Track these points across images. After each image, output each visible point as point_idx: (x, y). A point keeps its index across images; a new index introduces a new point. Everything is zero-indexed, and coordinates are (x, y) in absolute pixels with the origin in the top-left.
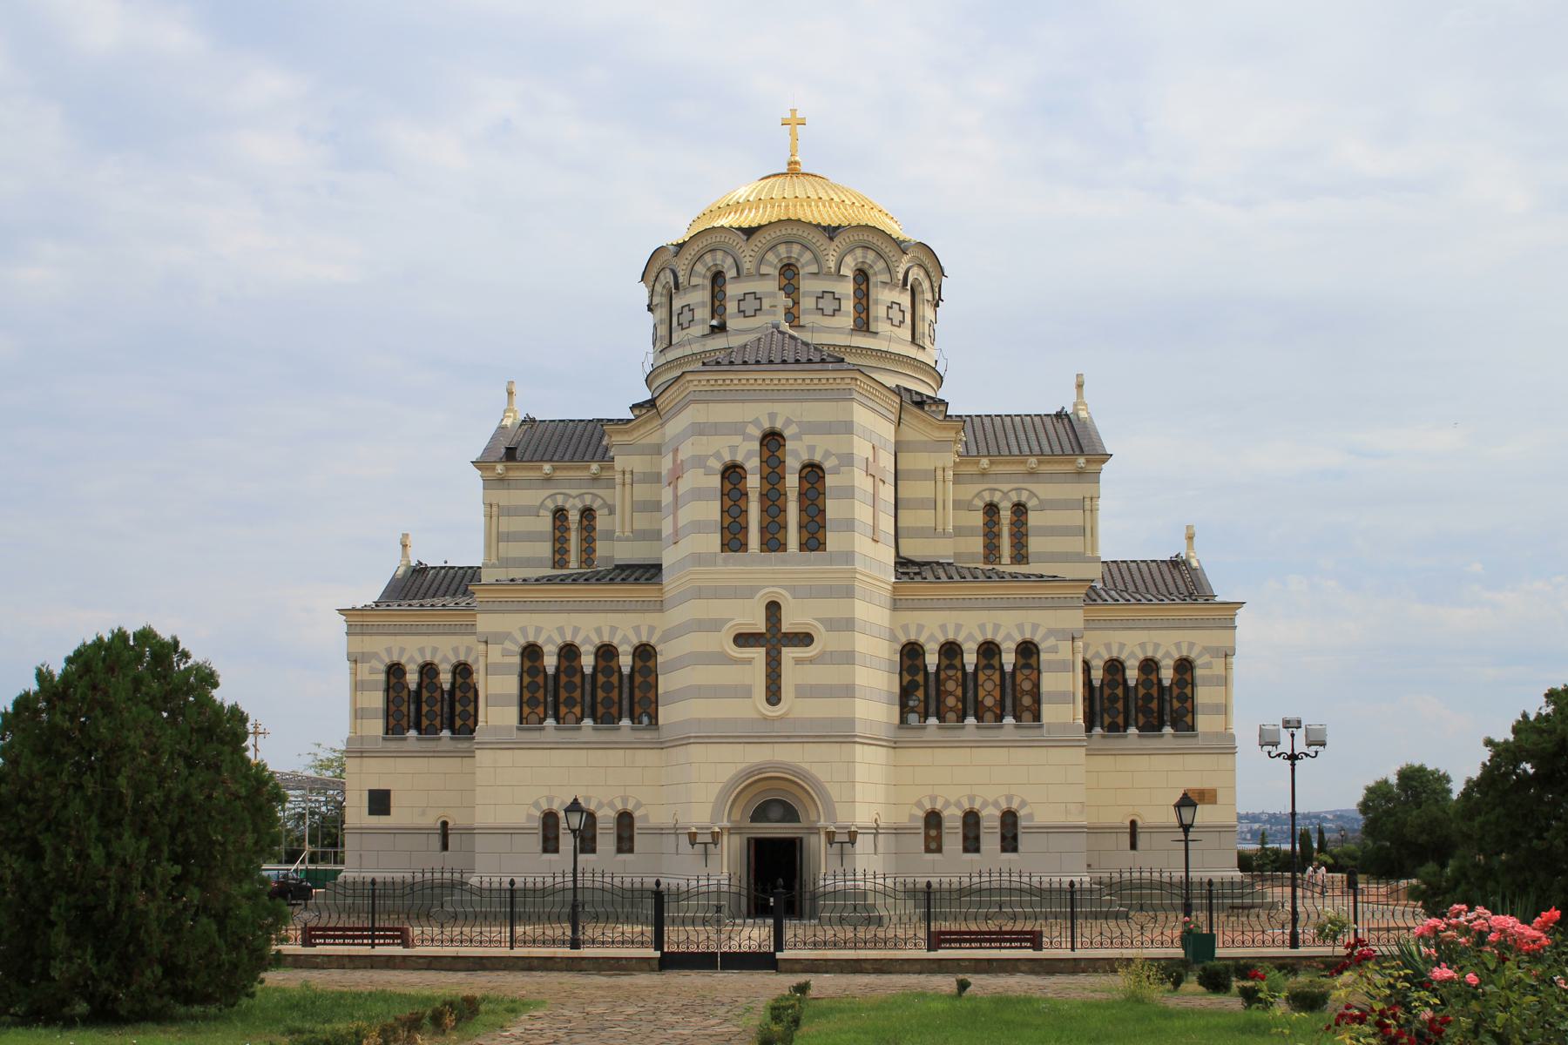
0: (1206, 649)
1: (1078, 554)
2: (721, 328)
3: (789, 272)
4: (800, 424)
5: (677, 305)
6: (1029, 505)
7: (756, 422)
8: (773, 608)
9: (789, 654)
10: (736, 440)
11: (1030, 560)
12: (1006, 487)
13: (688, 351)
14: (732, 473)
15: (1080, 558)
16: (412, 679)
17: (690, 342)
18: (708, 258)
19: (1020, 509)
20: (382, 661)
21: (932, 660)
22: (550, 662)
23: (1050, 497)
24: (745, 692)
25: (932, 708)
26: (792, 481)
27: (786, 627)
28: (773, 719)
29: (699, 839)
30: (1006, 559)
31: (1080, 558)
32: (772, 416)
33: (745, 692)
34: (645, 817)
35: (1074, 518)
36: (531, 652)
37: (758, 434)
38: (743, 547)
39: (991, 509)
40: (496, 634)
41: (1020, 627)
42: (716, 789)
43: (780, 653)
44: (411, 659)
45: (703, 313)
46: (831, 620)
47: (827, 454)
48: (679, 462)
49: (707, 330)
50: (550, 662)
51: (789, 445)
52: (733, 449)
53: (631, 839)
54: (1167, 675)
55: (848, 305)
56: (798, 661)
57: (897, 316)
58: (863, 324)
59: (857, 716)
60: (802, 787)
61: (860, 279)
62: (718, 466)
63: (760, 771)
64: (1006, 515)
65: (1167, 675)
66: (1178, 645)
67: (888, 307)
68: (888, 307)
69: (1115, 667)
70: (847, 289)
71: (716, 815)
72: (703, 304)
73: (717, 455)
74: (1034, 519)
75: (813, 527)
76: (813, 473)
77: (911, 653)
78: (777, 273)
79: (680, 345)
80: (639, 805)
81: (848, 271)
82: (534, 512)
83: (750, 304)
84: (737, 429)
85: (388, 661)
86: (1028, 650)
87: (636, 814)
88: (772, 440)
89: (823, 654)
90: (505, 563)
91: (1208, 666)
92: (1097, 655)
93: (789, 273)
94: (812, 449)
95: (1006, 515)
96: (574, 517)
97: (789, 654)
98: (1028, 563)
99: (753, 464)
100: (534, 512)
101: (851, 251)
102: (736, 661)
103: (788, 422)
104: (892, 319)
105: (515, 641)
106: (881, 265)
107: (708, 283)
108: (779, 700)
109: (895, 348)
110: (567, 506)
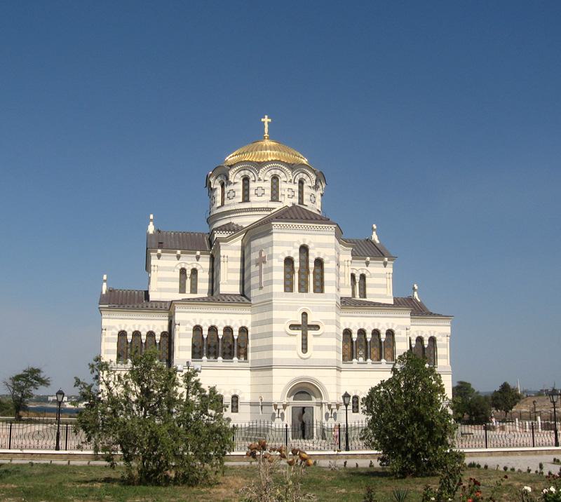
0: (440, 334)
1: (385, 295)
2: (248, 201)
3: (275, 178)
4: (314, 243)
5: (227, 189)
6: (367, 275)
7: (298, 242)
8: (305, 314)
9: (310, 333)
11: (367, 296)
13: (233, 208)
14: (289, 261)
16: (129, 337)
17: (234, 204)
19: (363, 277)
20: (116, 329)
21: (355, 336)
23: (374, 272)
24: (292, 348)
25: (354, 356)
26: (312, 265)
27: (309, 323)
28: (305, 359)
29: (278, 407)
31: (385, 296)
32: (304, 240)
33: (292, 348)
34: (243, 398)
36: (198, 329)
37: (299, 246)
38: (291, 290)
39: (353, 276)
41: (387, 324)
42: (284, 386)
43: (307, 333)
44: (130, 330)
45: (240, 194)
46: (327, 320)
47: (325, 255)
48: (263, 256)
49: (241, 200)
51: (310, 251)
52: (289, 252)
53: (237, 407)
54: (426, 343)
55: (297, 194)
56: (314, 336)
57: (313, 199)
59: (273, 357)
60: (316, 387)
61: (301, 184)
62: (283, 258)
63: (299, 380)
64: (358, 278)
65: (426, 343)
66: (430, 332)
69: (420, 339)
70: (296, 187)
71: (282, 397)
72: (238, 190)
73: (283, 254)
74: (368, 281)
75: (318, 284)
76: (319, 262)
77: (347, 332)
79: (228, 205)
80: (241, 392)
81: (297, 181)
82: (171, 269)
83: (260, 192)
84: (291, 244)
85: (119, 330)
86: (390, 333)
87: (240, 396)
88: (304, 249)
89: (323, 333)
90: (160, 290)
91: (441, 340)
92: (413, 335)
93: (275, 181)
95: (358, 278)
96: (189, 272)
97: (310, 333)
99: (296, 258)
100: (171, 269)
102: (290, 335)
103: (310, 242)
105: (191, 324)
106: (308, 179)
107: (241, 182)
108: (307, 351)
110: (186, 268)
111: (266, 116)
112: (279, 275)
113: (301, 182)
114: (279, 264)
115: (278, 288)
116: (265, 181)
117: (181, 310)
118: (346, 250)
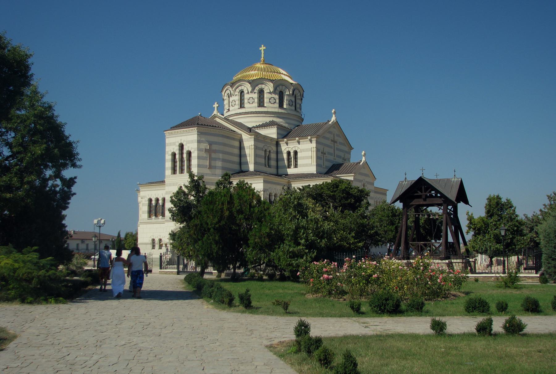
3: (242, 92)
10: (174, 147)
12: (292, 147)
14: (174, 155)
15: (311, 165)
18: (227, 91)
19: (296, 153)
22: (154, 202)
26: (185, 156)
30: (292, 167)
35: (309, 154)
37: (178, 144)
39: (289, 153)
40: (144, 196)
47: (192, 148)
50: (154, 202)
51: (185, 147)
55: (256, 100)
57: (272, 101)
58: (261, 103)
64: (292, 154)
67: (270, 99)
68: (270, 99)
70: (255, 96)
74: (299, 155)
76: (189, 153)
78: (239, 94)
81: (256, 91)
83: (234, 103)
84: (174, 144)
88: (181, 146)
94: (189, 147)
95: (292, 154)
98: (297, 167)
99: (177, 152)
101: (257, 85)
103: (184, 141)
104: (271, 102)
106: (266, 88)
107: (227, 98)
109: (270, 110)
111: (263, 46)
112: (168, 164)
113: (261, 92)
114: (168, 157)
115: (168, 172)
116: (236, 95)
117: (144, 190)
118: (251, 138)
